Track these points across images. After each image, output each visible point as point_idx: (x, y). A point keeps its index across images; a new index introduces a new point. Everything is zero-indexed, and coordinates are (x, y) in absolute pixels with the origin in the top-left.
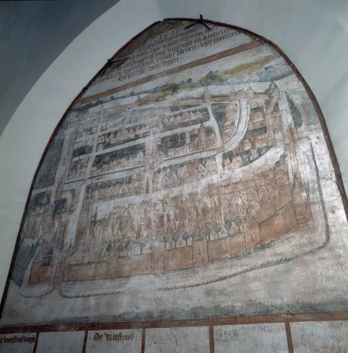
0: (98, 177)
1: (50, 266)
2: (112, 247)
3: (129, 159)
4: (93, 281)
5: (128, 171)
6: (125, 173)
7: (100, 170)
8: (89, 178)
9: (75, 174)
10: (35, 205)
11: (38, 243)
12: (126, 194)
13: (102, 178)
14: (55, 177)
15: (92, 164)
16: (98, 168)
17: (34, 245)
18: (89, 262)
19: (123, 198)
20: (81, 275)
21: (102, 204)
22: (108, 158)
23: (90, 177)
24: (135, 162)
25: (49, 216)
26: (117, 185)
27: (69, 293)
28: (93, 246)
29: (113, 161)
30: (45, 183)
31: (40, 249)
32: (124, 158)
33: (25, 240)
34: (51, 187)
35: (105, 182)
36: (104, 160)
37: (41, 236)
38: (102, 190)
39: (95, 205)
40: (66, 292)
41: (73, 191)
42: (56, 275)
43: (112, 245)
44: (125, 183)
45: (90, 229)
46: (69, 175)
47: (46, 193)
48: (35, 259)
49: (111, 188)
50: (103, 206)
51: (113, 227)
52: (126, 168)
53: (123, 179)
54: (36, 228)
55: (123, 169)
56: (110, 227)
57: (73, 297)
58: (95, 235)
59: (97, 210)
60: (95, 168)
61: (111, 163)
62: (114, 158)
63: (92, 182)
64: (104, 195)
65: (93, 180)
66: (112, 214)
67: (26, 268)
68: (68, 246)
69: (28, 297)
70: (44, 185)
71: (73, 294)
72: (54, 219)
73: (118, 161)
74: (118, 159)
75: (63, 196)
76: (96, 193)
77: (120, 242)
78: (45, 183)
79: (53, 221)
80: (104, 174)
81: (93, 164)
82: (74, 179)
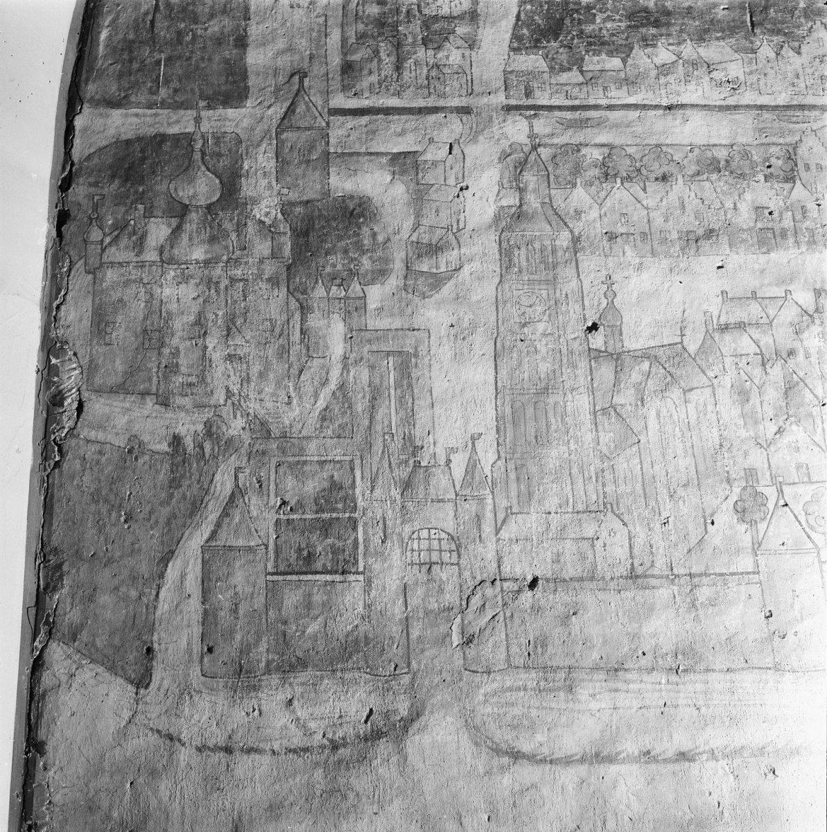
0: (568, 115)
1: (352, 578)
2: (771, 505)
3: (754, 51)
4: (692, 676)
5: (767, 115)
6: (746, 120)
7: (574, 76)
8: (508, 109)
9: (398, 68)
10: (119, 199)
11: (210, 431)
12: (784, 234)
13: (600, 124)
14: (242, 58)
15: (508, 36)
16: (556, 68)
17: (189, 442)
18: (633, 576)
19: (772, 255)
20: (598, 641)
21: (640, 267)
22: (609, 18)
23: (513, 102)
24: (798, 76)
25: (264, 285)
26: (714, 176)
27: (539, 738)
28: (639, 487)
29: (647, 42)
30: (175, 84)
31: (238, 470)
32: (722, 43)
33: (97, 407)
34: (231, 112)
35: (630, 150)
36: (589, 28)
37: (229, 394)
38: (620, 194)
39: (589, 262)
40: (514, 727)
41: (405, 163)
42: (415, 633)
43: (771, 493)
44: (761, 177)
45: (592, 391)
46: (348, 68)
47: (198, 145)
48: (218, 525)
49: (679, 187)
50: (645, 275)
51: (743, 395)
52: (748, 98)
53: (746, 155)
54: (175, 341)
55: (731, 101)
56: (724, 395)
57: (582, 760)
58: (637, 426)
59: (611, 294)
60: (532, 61)
61: (636, 50)
62: (653, 31)
63: (532, 136)
64: (638, 215)
65: (535, 122)
66: (725, 328)
67: (162, 576)
68: (458, 470)
69: (228, 750)
70: (163, 92)
71: (570, 743)
72: (304, 309)
73: (688, 50)
74: (679, 44)
75: (341, 183)
76: (580, 196)
77: (811, 483)
78: (175, 84)
79: (303, 321)
80: (610, 108)
81: (516, 37)
82: (398, 94)
